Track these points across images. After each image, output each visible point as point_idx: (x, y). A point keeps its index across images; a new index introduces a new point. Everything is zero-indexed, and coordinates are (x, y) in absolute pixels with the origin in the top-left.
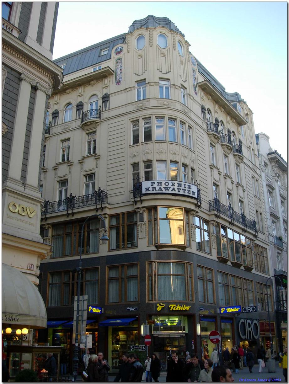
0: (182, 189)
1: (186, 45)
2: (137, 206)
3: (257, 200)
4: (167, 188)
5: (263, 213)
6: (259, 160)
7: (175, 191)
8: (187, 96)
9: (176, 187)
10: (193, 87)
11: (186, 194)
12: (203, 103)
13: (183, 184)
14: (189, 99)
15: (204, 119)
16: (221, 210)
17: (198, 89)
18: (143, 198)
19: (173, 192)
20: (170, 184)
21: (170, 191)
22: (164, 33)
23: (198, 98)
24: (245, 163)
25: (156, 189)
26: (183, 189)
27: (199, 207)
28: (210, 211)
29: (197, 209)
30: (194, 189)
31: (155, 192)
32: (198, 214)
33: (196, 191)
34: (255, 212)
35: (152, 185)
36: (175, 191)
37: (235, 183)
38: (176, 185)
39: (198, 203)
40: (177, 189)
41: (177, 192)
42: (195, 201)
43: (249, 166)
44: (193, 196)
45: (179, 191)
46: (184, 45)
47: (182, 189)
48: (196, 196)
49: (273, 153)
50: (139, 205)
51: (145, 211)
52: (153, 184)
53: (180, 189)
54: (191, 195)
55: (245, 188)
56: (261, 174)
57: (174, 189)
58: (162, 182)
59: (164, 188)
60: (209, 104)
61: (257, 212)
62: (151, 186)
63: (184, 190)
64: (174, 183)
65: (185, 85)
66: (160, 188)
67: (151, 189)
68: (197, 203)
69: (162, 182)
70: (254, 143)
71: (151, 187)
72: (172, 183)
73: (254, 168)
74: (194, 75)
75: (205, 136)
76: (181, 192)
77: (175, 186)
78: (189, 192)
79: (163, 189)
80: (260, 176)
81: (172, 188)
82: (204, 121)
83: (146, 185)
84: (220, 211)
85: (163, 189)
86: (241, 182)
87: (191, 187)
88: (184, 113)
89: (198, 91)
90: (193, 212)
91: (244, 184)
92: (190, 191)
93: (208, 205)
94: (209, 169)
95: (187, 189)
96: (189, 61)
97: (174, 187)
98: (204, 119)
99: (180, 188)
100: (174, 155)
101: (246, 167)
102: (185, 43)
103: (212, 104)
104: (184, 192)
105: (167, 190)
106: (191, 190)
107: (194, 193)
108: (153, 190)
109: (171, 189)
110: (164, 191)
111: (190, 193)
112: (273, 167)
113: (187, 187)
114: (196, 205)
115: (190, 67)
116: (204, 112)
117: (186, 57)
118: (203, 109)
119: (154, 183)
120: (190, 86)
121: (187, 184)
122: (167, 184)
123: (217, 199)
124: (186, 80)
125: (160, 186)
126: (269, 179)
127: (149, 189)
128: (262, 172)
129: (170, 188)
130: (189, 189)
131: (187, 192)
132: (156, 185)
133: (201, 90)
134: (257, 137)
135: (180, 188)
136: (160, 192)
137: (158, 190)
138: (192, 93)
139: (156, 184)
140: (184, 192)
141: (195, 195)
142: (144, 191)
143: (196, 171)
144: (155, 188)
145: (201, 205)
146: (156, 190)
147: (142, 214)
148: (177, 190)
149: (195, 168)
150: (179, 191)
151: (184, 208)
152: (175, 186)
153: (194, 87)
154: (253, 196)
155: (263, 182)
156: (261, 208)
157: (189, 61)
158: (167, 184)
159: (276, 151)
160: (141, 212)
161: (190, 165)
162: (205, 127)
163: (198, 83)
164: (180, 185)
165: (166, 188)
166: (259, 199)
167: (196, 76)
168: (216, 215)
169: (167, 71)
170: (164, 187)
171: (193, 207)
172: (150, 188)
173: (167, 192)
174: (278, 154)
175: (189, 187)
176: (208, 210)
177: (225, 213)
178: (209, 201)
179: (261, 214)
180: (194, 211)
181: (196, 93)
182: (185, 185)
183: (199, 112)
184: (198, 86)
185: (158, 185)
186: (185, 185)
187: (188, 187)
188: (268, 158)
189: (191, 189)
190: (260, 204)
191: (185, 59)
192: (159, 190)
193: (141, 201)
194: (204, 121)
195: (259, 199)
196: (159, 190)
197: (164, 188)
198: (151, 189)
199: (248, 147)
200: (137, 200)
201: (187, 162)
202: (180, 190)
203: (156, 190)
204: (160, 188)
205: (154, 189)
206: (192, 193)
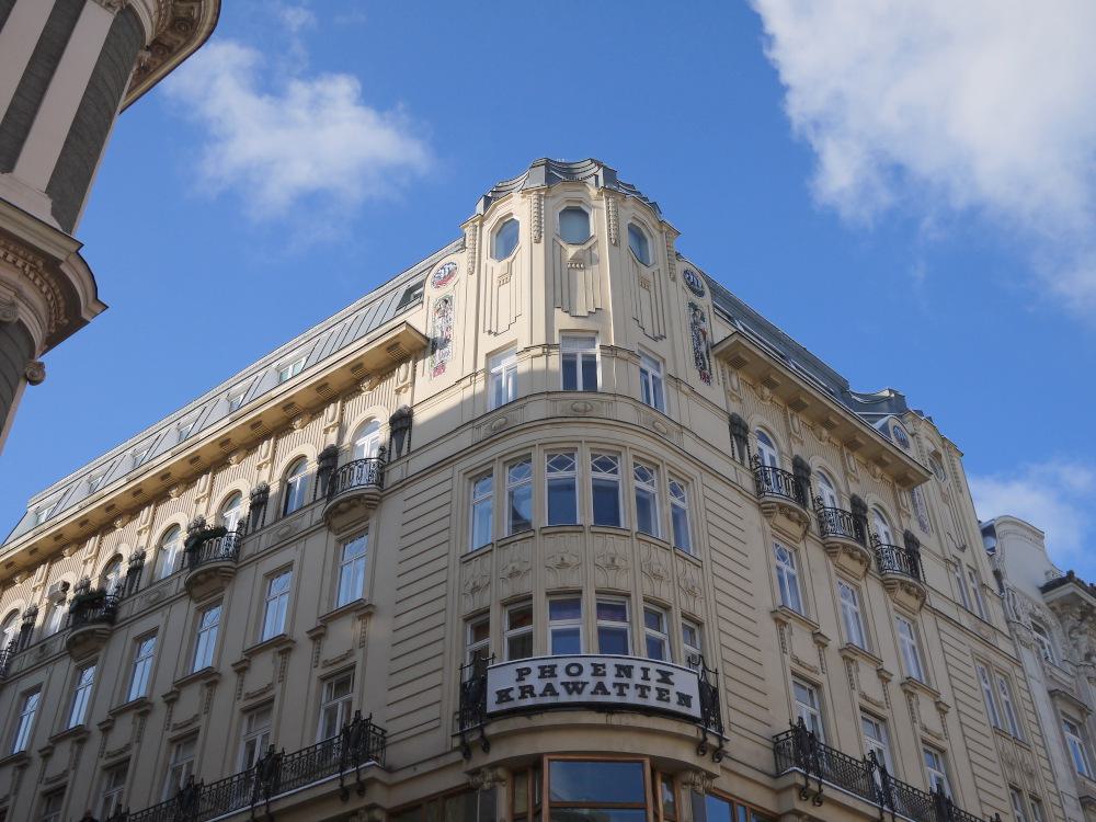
0: (632, 687)
1: (661, 232)
2: (472, 765)
3: (1009, 747)
4: (575, 684)
5: (1050, 800)
6: (1004, 608)
7: (606, 693)
8: (667, 383)
9: (610, 679)
10: (693, 359)
11: (652, 700)
12: (735, 408)
13: (637, 666)
14: (672, 391)
15: (742, 458)
16: (825, 766)
17: (715, 367)
18: (491, 730)
19: (600, 698)
20: (588, 670)
21: (586, 697)
22: (581, 202)
23: (715, 392)
24: (936, 612)
25: (535, 692)
26: (637, 686)
27: (718, 754)
28: (777, 776)
29: (705, 763)
30: (686, 683)
31: (529, 701)
32: (716, 783)
33: (693, 691)
34: (1005, 793)
35: (520, 679)
36: (606, 693)
37: (896, 679)
38: (611, 671)
39: (705, 739)
40: (615, 685)
41: (614, 698)
42: (691, 731)
43: (958, 625)
44: (683, 710)
45: (621, 694)
46: (656, 233)
47: (632, 687)
48: (695, 710)
49: (1061, 582)
50: (480, 760)
51: (501, 780)
52: (523, 673)
53: (627, 686)
54: (673, 705)
55: (946, 697)
56: (1018, 654)
57: (601, 688)
58: (556, 666)
59: (565, 684)
60: (761, 415)
61: (1016, 790)
62: (517, 680)
64: (604, 666)
65: (661, 348)
66: (550, 689)
67: (515, 694)
68: (701, 736)
69: (556, 666)
70: (975, 548)
71: (515, 685)
72: (592, 664)
73: (985, 631)
74: (696, 323)
75: (751, 514)
76: (632, 697)
77: (604, 674)
78: (662, 694)
80: (1017, 662)
81: (593, 682)
82: (742, 464)
83: (501, 678)
84: (819, 773)
85: (560, 689)
86: (928, 679)
87: (671, 678)
88: (652, 434)
89: (713, 369)
90: (691, 776)
91: (941, 684)
92: (667, 692)
93: (772, 753)
94: (772, 626)
95: (653, 684)
96: (674, 279)
97: (601, 679)
98: (742, 458)
99: (624, 680)
100: (611, 573)
101: (942, 624)
102: (657, 227)
103: (778, 415)
104: (643, 695)
105: (575, 693)
106: (673, 691)
107: (685, 699)
108: (523, 696)
109: (590, 687)
110: (564, 697)
111: (668, 700)
112: (1070, 633)
113: (654, 675)
114: (701, 747)
115: (679, 296)
116: (741, 437)
117: (661, 266)
118: (738, 429)
119: (529, 671)
120: (679, 353)
121: (653, 667)
122: (574, 670)
123: (804, 727)
124: (662, 333)
125: (548, 680)
126: (1062, 675)
127: (512, 694)
128: (1024, 651)
129: (584, 684)
130: (664, 686)
131: (653, 694)
132: (532, 679)
133: (727, 369)
134: (988, 531)
135: (624, 680)
136: (549, 700)
137: (541, 695)
138: (693, 377)
139: (536, 672)
140: (643, 695)
141: (689, 706)
142: (492, 706)
143: (711, 632)
144: (531, 687)
145: (721, 746)
146: (533, 695)
147: (492, 791)
148: (614, 691)
149: (700, 613)
150: (621, 694)
151: (647, 761)
152: (604, 674)
153: (697, 359)
154: (988, 731)
155: (1033, 682)
156: (1031, 775)
157: (674, 279)
158: (574, 670)
159: (1071, 574)
160: (486, 786)
161: (681, 603)
162: (747, 482)
163: (714, 346)
164: (625, 671)
165: (571, 686)
166: (1020, 743)
167: (703, 325)
168: (803, 792)
170: (562, 684)
171: (686, 755)
172: (512, 689)
173: (575, 698)
174: (1080, 583)
175: (665, 677)
176: (772, 771)
177: (845, 782)
178: (775, 740)
179: (1037, 800)
180: (697, 770)
181: (706, 378)
182: (645, 670)
183: (721, 435)
184: (716, 356)
186: (645, 670)
187: (659, 676)
188: (1048, 604)
189: (673, 684)
190: (1028, 759)
191: (656, 273)
192: (542, 695)
193: (486, 744)
194: (742, 464)
195: (1020, 743)
196: (542, 695)
197: (565, 684)
198: (515, 694)
199: (946, 560)
200: (471, 740)
201: (665, 593)
202: (626, 691)
203: (533, 695)
204: (550, 689)
205: (527, 691)
206: (674, 698)
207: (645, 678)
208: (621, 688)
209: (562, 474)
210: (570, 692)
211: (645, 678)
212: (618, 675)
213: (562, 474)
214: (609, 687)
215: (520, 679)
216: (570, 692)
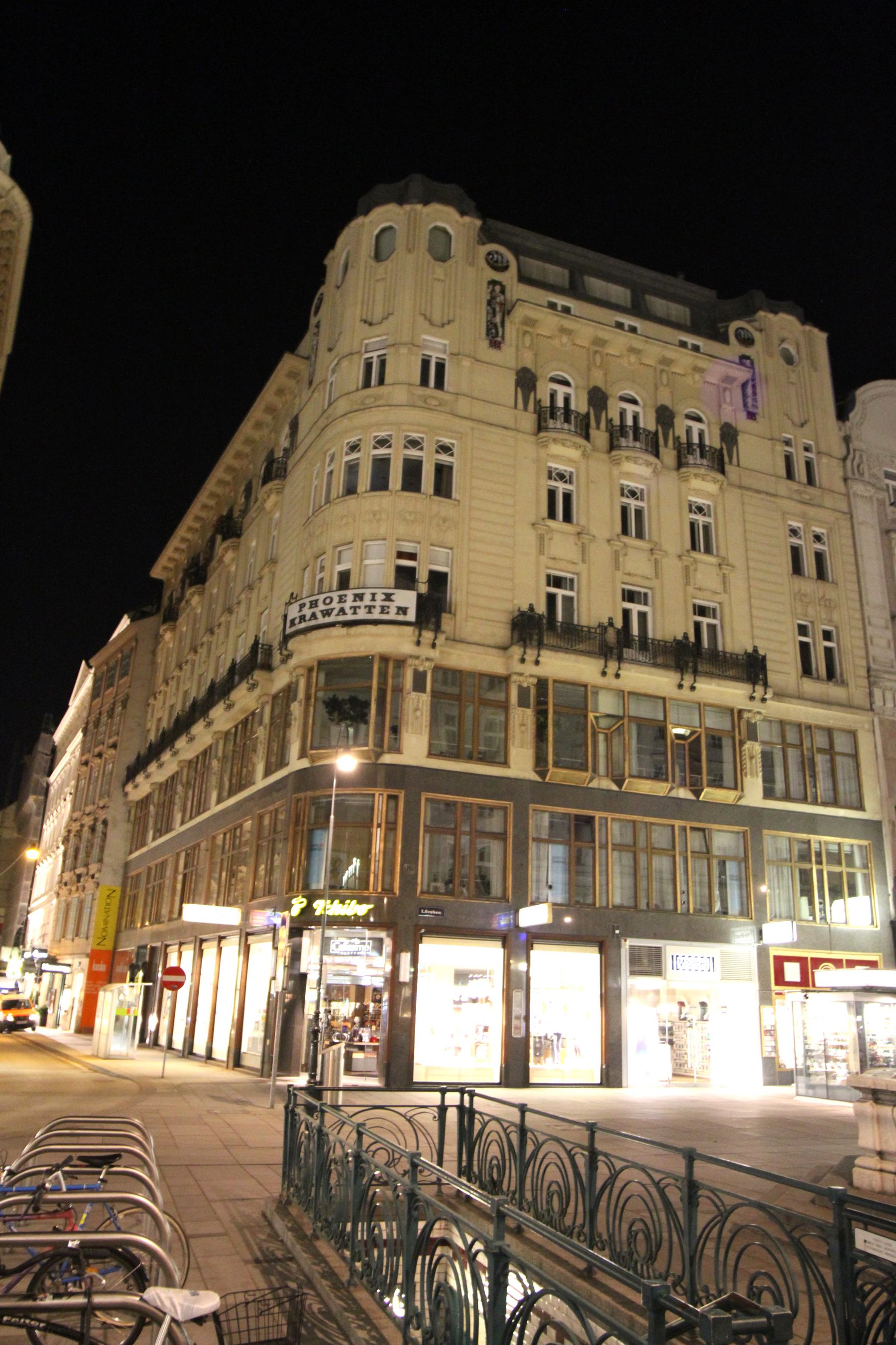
4: (327, 610)
19: (342, 618)
20: (336, 599)
35: (300, 610)
41: (350, 617)
45: (355, 613)
53: (359, 607)
57: (342, 611)
63: (370, 609)
76: (362, 615)
78: (383, 610)
79: (319, 615)
95: (379, 603)
99: (358, 603)
109: (335, 612)
110: (321, 620)
113: (380, 597)
119: (304, 605)
129: (333, 609)
135: (358, 603)
169: (445, 321)
173: (327, 620)
182: (374, 595)
185: (311, 607)
186: (374, 595)
204: (314, 616)
205: (303, 618)
207: (373, 599)
208: (355, 609)
209: (382, 451)
210: (324, 616)
211: (373, 599)
212: (355, 601)
213: (382, 451)
214: (348, 610)
215: (300, 610)
216: (324, 616)
